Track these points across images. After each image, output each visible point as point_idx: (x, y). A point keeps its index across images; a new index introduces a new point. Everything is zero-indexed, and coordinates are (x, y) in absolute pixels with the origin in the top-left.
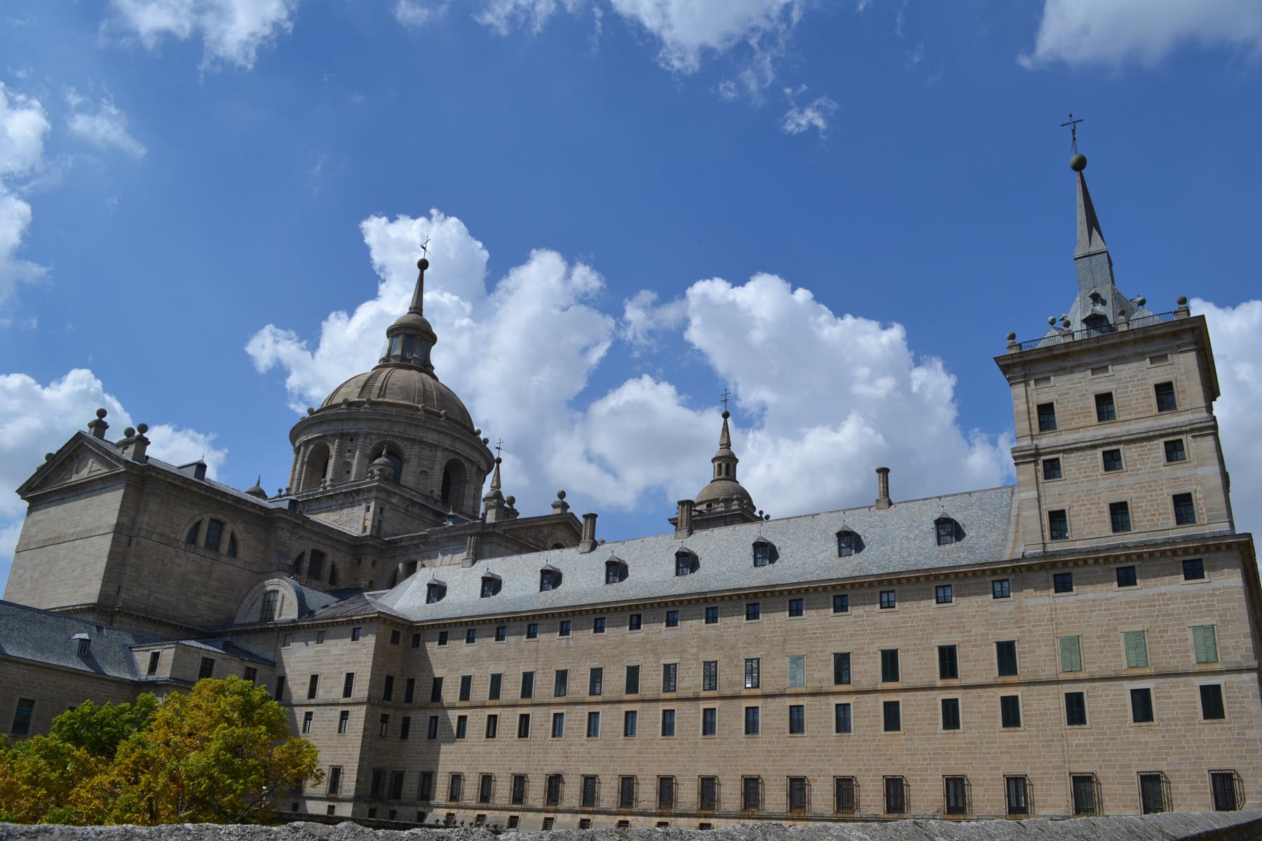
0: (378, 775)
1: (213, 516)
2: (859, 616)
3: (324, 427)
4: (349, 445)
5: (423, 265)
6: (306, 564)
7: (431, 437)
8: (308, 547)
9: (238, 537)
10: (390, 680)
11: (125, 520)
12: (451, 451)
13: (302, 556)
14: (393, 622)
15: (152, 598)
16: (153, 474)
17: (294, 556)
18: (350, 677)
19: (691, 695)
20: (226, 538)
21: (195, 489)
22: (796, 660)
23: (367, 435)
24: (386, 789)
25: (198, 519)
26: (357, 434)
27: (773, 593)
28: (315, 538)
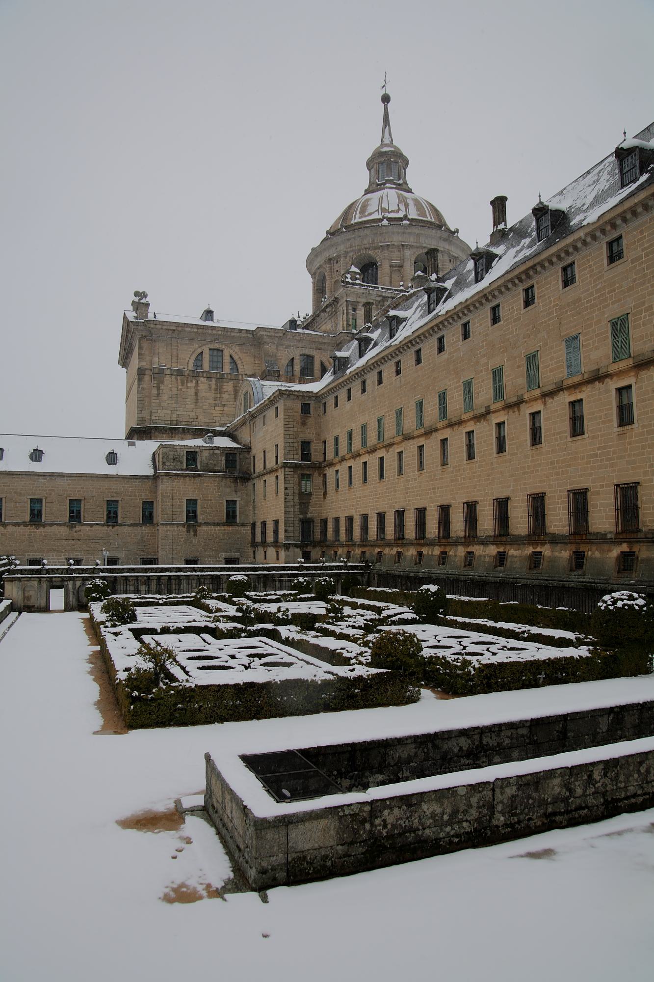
0: (306, 524)
1: (212, 346)
2: (640, 257)
3: (319, 259)
4: (336, 267)
5: (386, 99)
6: (297, 368)
7: (397, 239)
8: (296, 353)
9: (236, 357)
10: (306, 445)
11: (144, 364)
12: (417, 247)
13: (293, 359)
14: (298, 396)
15: (175, 416)
16: (152, 326)
17: (285, 362)
18: (277, 446)
19: (483, 410)
20: (227, 359)
21: (188, 329)
22: (572, 341)
23: (346, 253)
24: (317, 535)
25: (199, 351)
26: (339, 256)
27: (541, 264)
28: (300, 345)
